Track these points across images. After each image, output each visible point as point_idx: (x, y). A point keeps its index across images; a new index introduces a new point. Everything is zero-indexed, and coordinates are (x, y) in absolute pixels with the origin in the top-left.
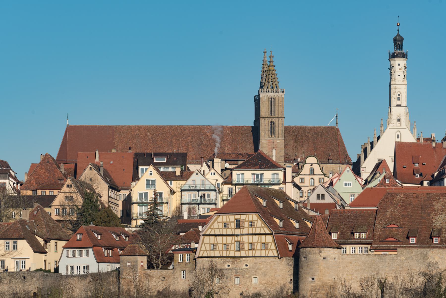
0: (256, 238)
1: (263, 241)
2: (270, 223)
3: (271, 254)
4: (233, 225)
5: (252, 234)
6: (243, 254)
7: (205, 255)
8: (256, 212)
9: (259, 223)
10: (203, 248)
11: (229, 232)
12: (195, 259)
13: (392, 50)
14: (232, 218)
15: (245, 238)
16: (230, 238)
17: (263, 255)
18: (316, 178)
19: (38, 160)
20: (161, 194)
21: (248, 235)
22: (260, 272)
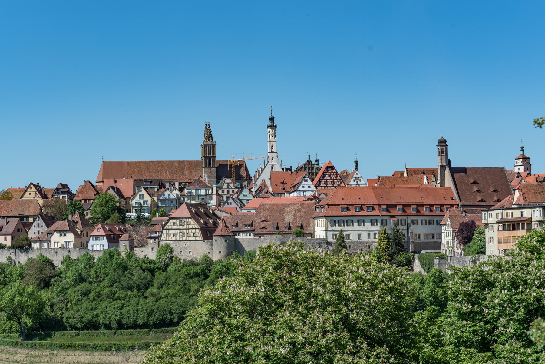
0: (190, 231)
1: (194, 232)
2: (198, 222)
3: (198, 239)
4: (178, 223)
5: (188, 229)
6: (184, 239)
7: (164, 239)
8: (190, 218)
9: (192, 223)
10: (163, 236)
11: (176, 227)
12: (159, 242)
13: (269, 124)
14: (178, 220)
15: (185, 231)
16: (177, 231)
17: (194, 239)
18: (230, 190)
19: (83, 184)
20: (147, 202)
21: (186, 229)
22: (193, 248)
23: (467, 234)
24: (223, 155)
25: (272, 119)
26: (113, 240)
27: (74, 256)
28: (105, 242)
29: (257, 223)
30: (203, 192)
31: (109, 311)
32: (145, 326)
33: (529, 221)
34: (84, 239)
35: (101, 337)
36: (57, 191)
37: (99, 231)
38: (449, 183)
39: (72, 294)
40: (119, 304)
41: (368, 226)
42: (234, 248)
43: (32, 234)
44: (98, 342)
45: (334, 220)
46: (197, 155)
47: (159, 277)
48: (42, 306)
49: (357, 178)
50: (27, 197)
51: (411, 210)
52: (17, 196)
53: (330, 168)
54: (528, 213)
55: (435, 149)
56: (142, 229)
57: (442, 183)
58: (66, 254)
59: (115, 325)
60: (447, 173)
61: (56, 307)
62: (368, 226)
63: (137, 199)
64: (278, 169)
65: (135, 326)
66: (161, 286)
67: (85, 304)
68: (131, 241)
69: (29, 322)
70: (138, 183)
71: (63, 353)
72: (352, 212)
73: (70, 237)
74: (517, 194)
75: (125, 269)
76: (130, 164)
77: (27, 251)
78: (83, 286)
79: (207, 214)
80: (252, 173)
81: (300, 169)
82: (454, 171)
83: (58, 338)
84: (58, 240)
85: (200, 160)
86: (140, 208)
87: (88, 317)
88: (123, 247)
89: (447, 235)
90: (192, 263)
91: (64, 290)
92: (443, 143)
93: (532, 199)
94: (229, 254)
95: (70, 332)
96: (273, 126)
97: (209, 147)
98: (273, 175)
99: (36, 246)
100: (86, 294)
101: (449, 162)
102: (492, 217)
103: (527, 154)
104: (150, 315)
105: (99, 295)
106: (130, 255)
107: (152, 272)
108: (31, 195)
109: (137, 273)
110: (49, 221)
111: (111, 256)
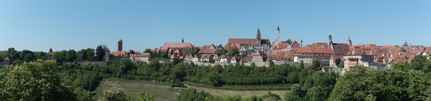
23: (338, 62)
24: (263, 37)
25: (278, 28)
26: (238, 61)
27: (227, 65)
28: (235, 61)
29: (277, 57)
30: (259, 48)
31: (238, 80)
32: (248, 84)
33: (358, 59)
34: (229, 60)
35: (236, 87)
36: (219, 47)
37: (234, 58)
38: (332, 47)
39: (228, 75)
40: (241, 78)
41: (309, 59)
42: (272, 63)
43: (214, 58)
44: (236, 88)
45: (299, 57)
46: (255, 37)
47: (252, 71)
48: (220, 77)
49: (302, 45)
50: (211, 48)
51: (321, 55)
52: (207, 47)
53: (295, 42)
54: (357, 57)
55: (328, 38)
56: (245, 58)
57: (330, 47)
58: (225, 64)
59: (240, 84)
60: (331, 44)
61: (223, 78)
62: (309, 59)
63: (241, 49)
64: (280, 42)
65: (246, 84)
66: (252, 74)
67: (231, 78)
68: (243, 61)
69: (216, 82)
70: (241, 45)
71: (226, 91)
72: (305, 55)
73: (226, 59)
74: (353, 51)
75: (242, 69)
76: (236, 39)
77: (213, 63)
78: (231, 73)
79: (264, 54)
80: (271, 43)
81: (286, 42)
82: (333, 44)
83: (224, 87)
84: (222, 60)
85: (256, 38)
86: (243, 52)
87: (232, 81)
88: (241, 63)
89: (332, 62)
90: (261, 68)
91: (225, 74)
92: (330, 36)
93: (358, 53)
94: (271, 65)
95: (227, 85)
96: (279, 30)
97: (259, 35)
98: (279, 43)
99: (216, 62)
100: (232, 75)
101: (332, 42)
102: (347, 57)
103: (350, 39)
104: (250, 81)
105: (235, 75)
106: (243, 65)
107: (250, 69)
108: (212, 47)
109: (245, 70)
110: (219, 55)
111: (238, 65)
